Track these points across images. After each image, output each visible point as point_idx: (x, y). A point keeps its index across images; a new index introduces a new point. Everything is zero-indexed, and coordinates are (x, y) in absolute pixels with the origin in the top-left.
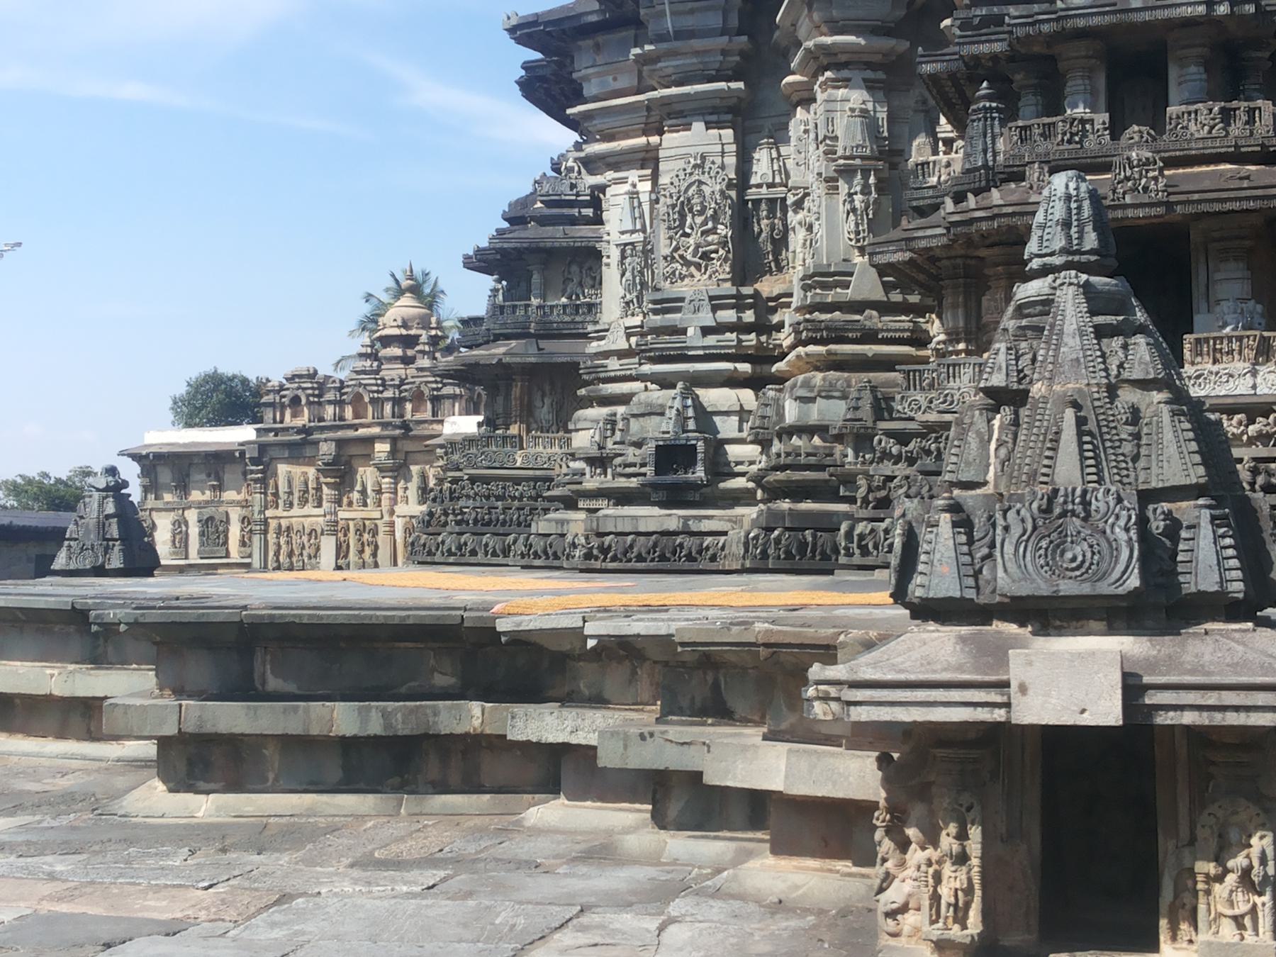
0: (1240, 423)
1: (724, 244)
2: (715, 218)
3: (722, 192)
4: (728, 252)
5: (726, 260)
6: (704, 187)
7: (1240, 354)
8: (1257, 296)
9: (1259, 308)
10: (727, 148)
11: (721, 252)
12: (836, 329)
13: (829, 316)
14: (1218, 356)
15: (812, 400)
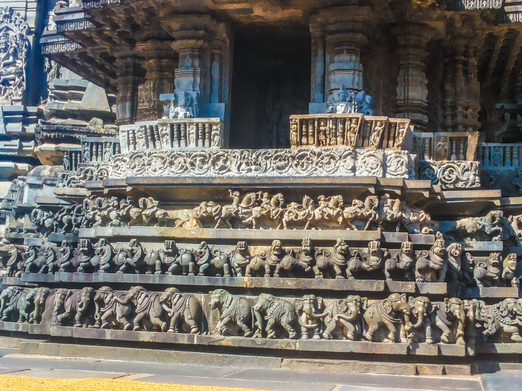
0: (337, 205)
1: (20, 74)
2: (15, 54)
3: (21, 36)
4: (23, 80)
5: (20, 86)
6: (10, 32)
7: (343, 136)
8: (367, 88)
9: (368, 98)
10: (30, 5)
11: (17, 80)
12: (65, 131)
13: (63, 121)
14: (322, 137)
15: (40, 187)
